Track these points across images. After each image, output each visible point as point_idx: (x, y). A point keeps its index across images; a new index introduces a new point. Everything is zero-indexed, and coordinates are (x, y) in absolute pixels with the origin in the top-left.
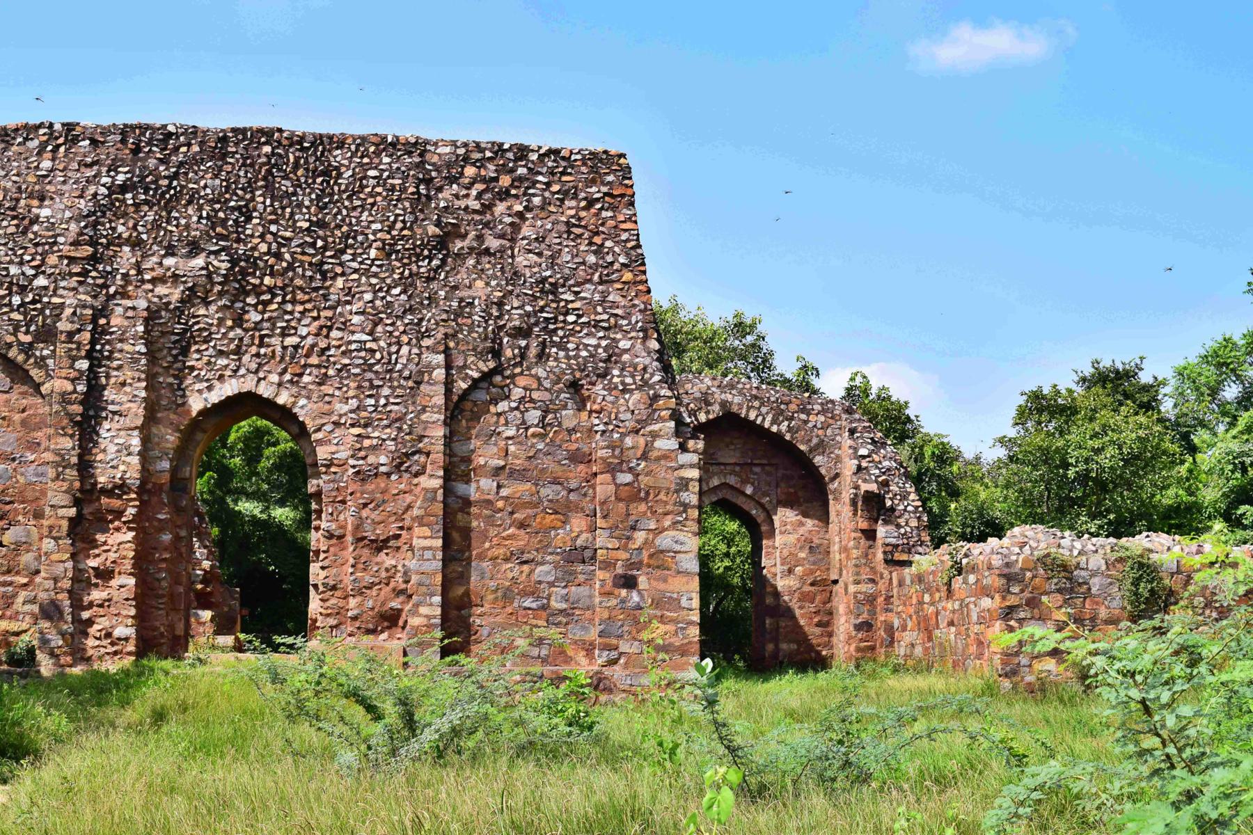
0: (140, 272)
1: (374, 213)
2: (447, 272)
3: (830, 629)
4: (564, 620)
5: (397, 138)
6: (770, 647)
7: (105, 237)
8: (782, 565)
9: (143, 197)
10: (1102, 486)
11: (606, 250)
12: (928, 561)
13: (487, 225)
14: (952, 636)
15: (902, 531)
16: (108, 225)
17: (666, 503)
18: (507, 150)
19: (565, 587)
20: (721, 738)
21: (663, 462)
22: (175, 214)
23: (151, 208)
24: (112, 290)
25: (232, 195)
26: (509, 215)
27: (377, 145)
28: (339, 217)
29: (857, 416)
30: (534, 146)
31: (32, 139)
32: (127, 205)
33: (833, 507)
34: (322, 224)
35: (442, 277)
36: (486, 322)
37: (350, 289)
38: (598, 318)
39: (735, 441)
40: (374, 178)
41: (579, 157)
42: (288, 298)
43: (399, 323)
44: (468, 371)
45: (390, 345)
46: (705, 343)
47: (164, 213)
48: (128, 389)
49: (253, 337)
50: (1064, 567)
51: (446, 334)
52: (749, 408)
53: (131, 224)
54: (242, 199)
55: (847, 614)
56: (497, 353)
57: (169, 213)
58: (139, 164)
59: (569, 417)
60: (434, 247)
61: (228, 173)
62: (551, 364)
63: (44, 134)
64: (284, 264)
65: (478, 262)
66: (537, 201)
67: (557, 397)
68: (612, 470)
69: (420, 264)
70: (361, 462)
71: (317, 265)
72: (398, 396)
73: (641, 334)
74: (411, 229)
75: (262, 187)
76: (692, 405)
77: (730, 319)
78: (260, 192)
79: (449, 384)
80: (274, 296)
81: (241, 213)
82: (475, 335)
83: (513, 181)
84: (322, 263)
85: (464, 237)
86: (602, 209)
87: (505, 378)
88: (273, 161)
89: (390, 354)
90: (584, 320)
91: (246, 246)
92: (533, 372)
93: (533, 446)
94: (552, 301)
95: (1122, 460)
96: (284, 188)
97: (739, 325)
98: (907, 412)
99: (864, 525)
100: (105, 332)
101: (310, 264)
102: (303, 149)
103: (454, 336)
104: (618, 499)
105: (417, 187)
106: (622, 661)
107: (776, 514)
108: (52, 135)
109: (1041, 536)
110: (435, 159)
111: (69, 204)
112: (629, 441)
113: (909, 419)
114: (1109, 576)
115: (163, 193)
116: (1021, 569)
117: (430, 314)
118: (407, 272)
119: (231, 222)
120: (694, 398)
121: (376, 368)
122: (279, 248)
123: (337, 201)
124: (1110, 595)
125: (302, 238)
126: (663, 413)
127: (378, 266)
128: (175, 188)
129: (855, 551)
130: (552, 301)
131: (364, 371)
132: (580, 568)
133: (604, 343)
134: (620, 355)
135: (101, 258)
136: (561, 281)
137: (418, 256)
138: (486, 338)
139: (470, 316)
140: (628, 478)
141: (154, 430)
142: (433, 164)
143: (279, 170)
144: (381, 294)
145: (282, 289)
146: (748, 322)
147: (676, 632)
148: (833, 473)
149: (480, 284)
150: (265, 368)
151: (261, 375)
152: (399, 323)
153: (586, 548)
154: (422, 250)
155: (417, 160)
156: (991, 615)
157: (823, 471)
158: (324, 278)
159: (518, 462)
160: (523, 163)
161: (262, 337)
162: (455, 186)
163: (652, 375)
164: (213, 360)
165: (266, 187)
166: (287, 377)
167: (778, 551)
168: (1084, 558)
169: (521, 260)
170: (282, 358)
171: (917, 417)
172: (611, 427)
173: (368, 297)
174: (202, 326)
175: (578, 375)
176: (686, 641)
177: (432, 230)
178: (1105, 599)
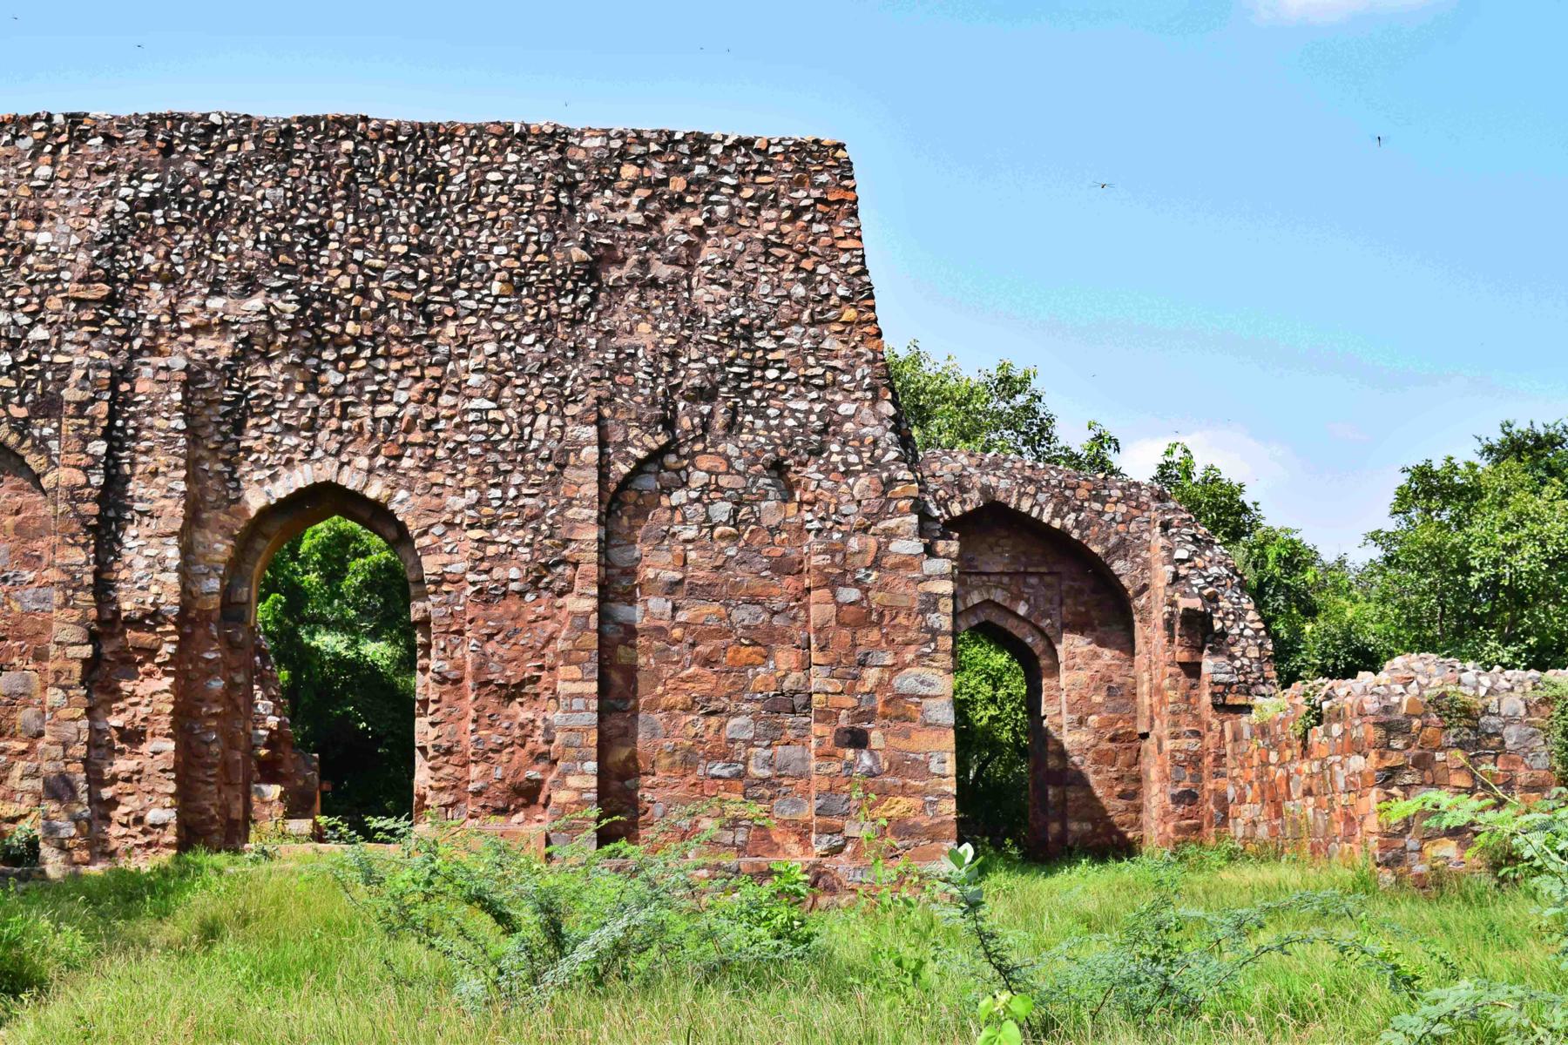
0: (175, 318)
1: (496, 232)
2: (600, 312)
3: (1137, 802)
4: (768, 793)
5: (527, 127)
6: (1055, 827)
7: (127, 270)
8: (1070, 712)
9: (178, 214)
10: (1518, 599)
11: (819, 278)
12: (1272, 705)
13: (653, 246)
14: (1310, 811)
15: (1238, 664)
16: (130, 254)
17: (907, 628)
18: (679, 142)
19: (769, 746)
20: (988, 955)
21: (901, 572)
22: (222, 237)
23: (189, 229)
24: (137, 344)
25: (300, 209)
26: (684, 232)
27: (499, 137)
28: (449, 238)
29: (1172, 505)
30: (717, 135)
31: (23, 137)
32: (155, 226)
33: (1140, 631)
34: (425, 248)
35: (592, 319)
36: (654, 380)
37: (465, 337)
38: (809, 372)
39: (1002, 542)
40: (496, 183)
41: (779, 149)
42: (380, 350)
43: (533, 383)
44: (629, 449)
45: (521, 414)
46: (958, 405)
47: (207, 237)
48: (160, 480)
49: (332, 406)
50: (1467, 712)
51: (598, 398)
52: (1021, 495)
53: (161, 252)
54: (314, 214)
55: (1161, 781)
56: (669, 424)
57: (214, 236)
58: (172, 169)
59: (771, 513)
60: (581, 278)
61: (294, 179)
62: (744, 437)
63: (40, 130)
64: (374, 305)
65: (642, 298)
66: (722, 211)
67: (754, 483)
68: (831, 583)
69: (562, 301)
70: (484, 577)
71: (418, 305)
72: (533, 485)
73: (869, 395)
74: (548, 252)
75: (341, 198)
76: (941, 493)
77: (993, 372)
78: (339, 205)
79: (603, 467)
80: (360, 348)
81: (313, 235)
82: (639, 399)
83: (689, 184)
84: (426, 302)
85: (622, 262)
86: (812, 221)
87: (680, 457)
88: (356, 162)
89: (521, 427)
90: (790, 375)
91: (320, 279)
92: (720, 449)
93: (721, 551)
94: (745, 350)
95: (1547, 561)
96: (371, 199)
97: (1006, 380)
98: (1242, 498)
99: (1183, 656)
100: (128, 402)
101: (410, 304)
102: (397, 145)
103: (610, 400)
104: (841, 624)
105: (556, 195)
106: (849, 849)
107: (1060, 642)
108: (50, 131)
109: (1432, 668)
110: (580, 155)
111: (76, 225)
112: (854, 543)
113: (1244, 508)
114: (1530, 724)
115: (206, 209)
116: (1406, 715)
117: (576, 371)
118: (543, 313)
119: (299, 248)
120: (945, 483)
121: (503, 446)
122: (366, 283)
123: (446, 216)
124: (1531, 750)
125: (397, 268)
126: (902, 504)
127: (503, 305)
128: (221, 201)
129: (1171, 693)
130: (745, 350)
131: (486, 451)
132: (790, 719)
133: (818, 407)
134: (841, 424)
135: (122, 300)
136: (757, 322)
137: (558, 290)
138: (654, 403)
139: (632, 372)
140: (851, 594)
141: (198, 537)
142: (578, 163)
143: (365, 174)
144: (508, 344)
145: (371, 338)
146: (1019, 375)
147: (924, 808)
148: (1139, 584)
149: (644, 327)
150: (350, 449)
151: (344, 458)
152: (533, 383)
153: (797, 692)
154: (564, 282)
155: (555, 157)
156: (1364, 780)
157: (1125, 582)
158: (429, 323)
159: (701, 574)
160: (703, 159)
161: (344, 406)
162: (608, 193)
163: (886, 451)
164: (277, 438)
165: (346, 197)
166: (380, 460)
167: (1064, 694)
168: (1495, 699)
169: (702, 294)
170: (373, 435)
171: (1256, 504)
172: (829, 524)
173: (490, 348)
174: (261, 391)
175: (782, 452)
176: (937, 820)
177: (578, 254)
178: (1526, 756)
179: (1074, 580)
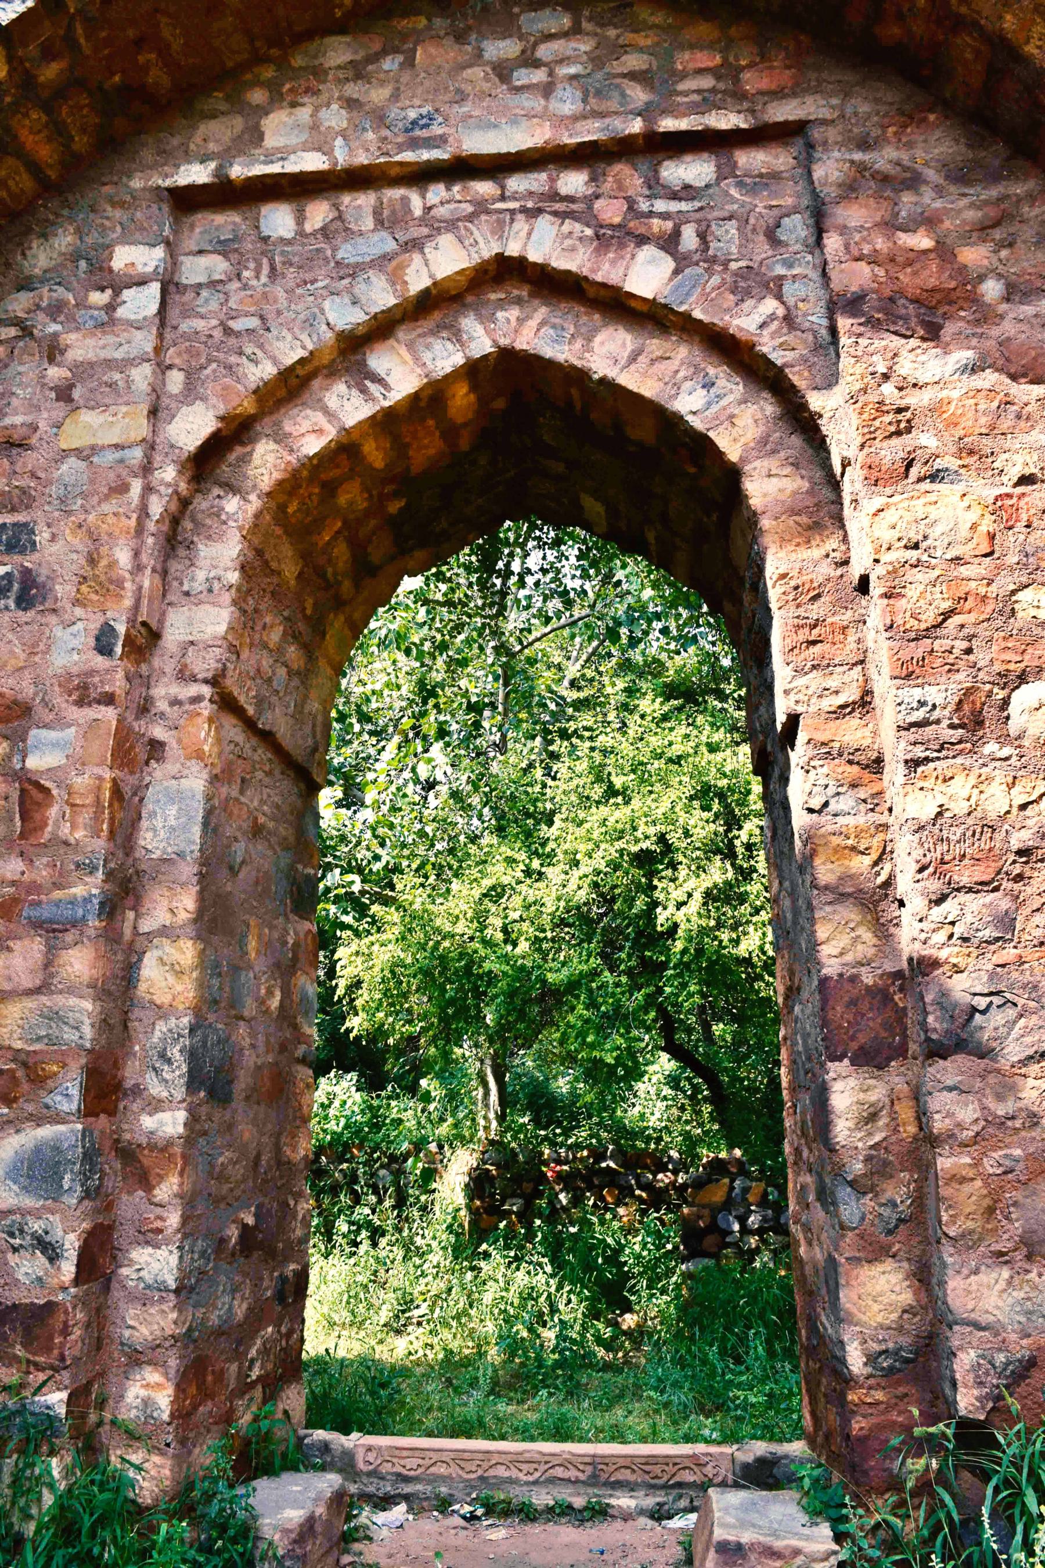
39: (544, 51)
107: (831, 381)
179: (864, 144)
